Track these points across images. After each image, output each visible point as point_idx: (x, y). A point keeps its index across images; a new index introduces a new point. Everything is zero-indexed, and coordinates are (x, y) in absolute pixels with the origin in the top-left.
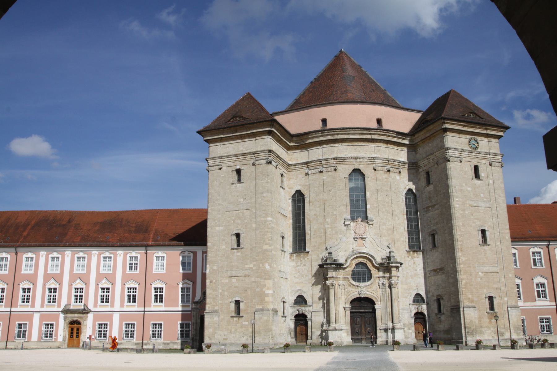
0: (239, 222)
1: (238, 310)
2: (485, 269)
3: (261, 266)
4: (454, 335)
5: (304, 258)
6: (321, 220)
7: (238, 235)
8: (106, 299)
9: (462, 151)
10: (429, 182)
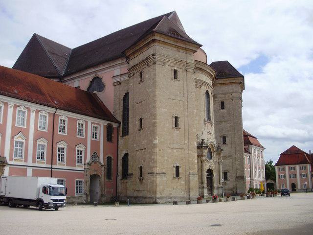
0: (177, 109)
1: (177, 174)
7: (176, 118)
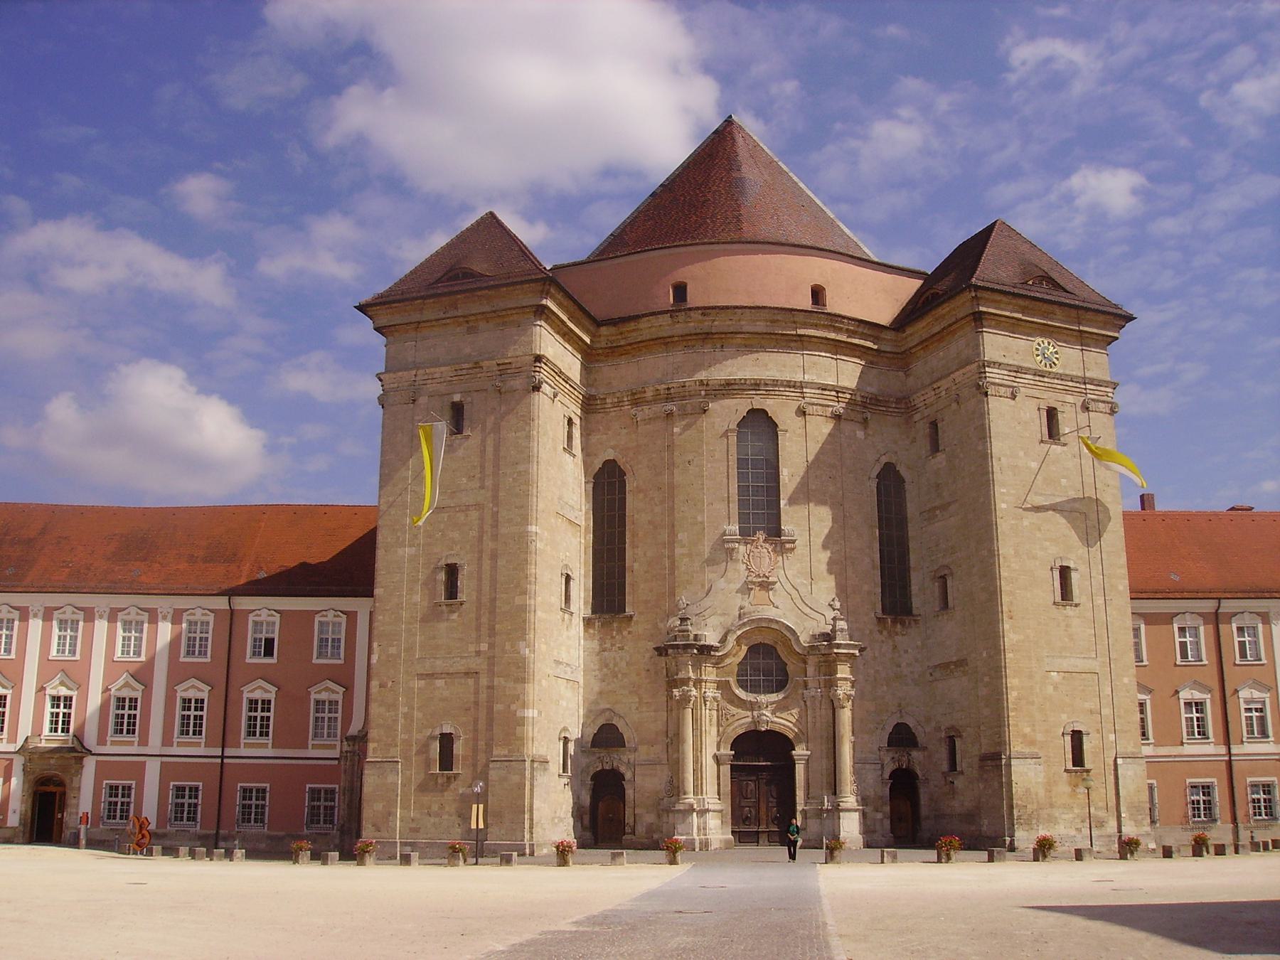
0: (456, 535)
2: (1066, 664)
3: (508, 647)
4: (986, 825)
5: (619, 631)
6: (664, 536)
8: (126, 725)
9: (1019, 370)
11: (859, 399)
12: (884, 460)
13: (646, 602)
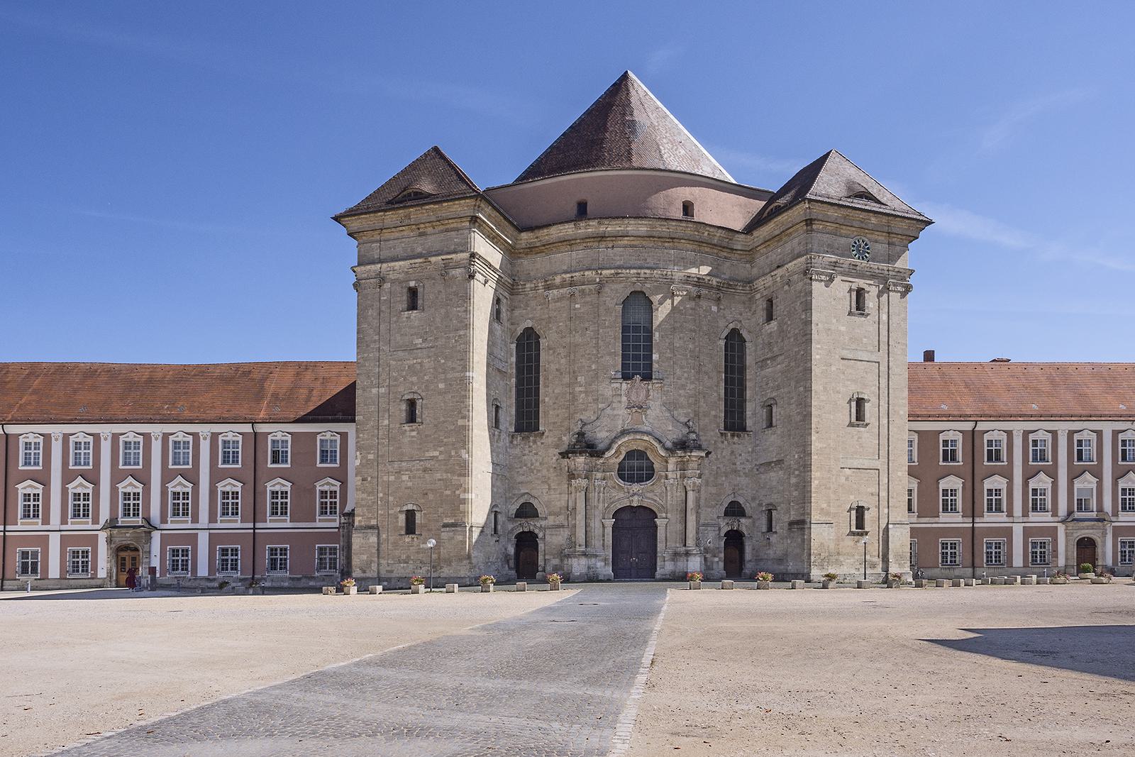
10: (770, 318)
11: (715, 283)
12: (731, 326)
13: (554, 423)
